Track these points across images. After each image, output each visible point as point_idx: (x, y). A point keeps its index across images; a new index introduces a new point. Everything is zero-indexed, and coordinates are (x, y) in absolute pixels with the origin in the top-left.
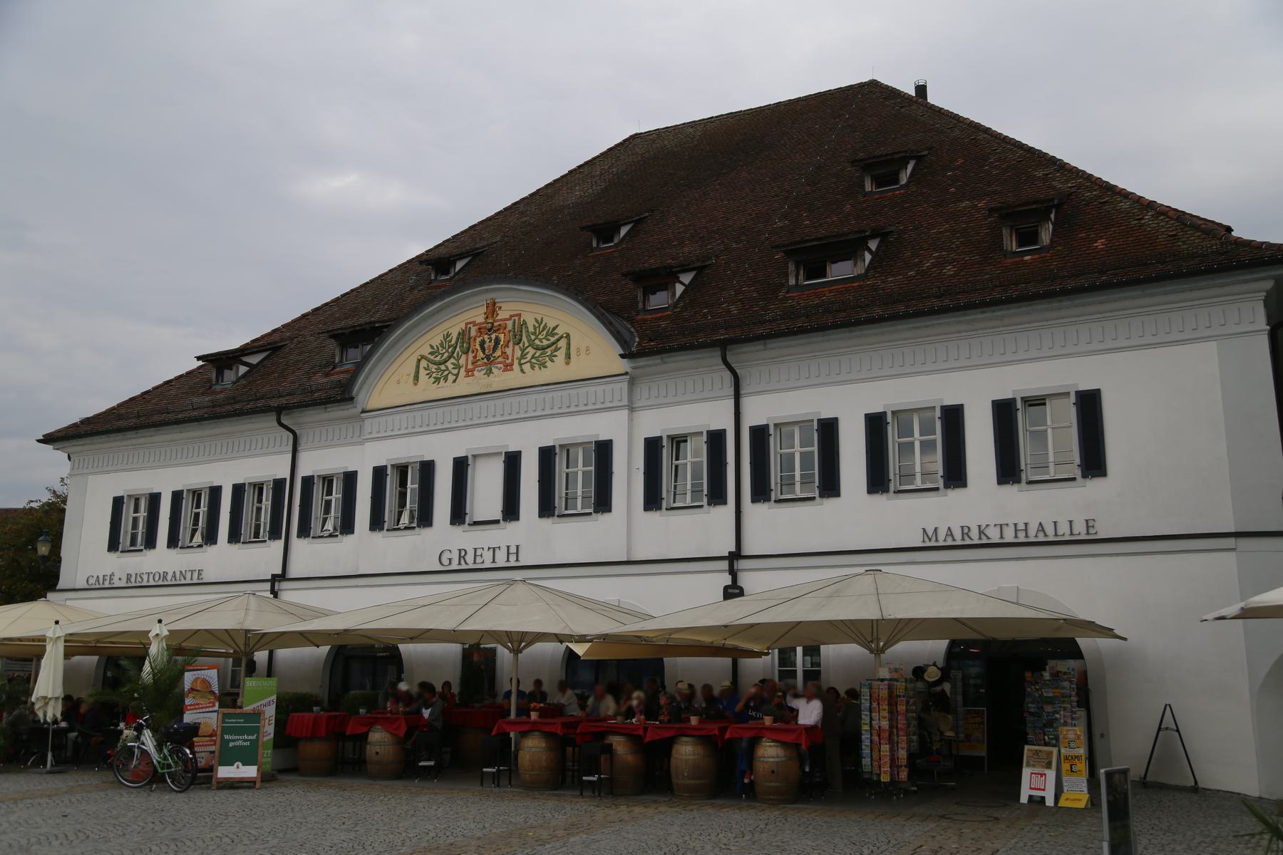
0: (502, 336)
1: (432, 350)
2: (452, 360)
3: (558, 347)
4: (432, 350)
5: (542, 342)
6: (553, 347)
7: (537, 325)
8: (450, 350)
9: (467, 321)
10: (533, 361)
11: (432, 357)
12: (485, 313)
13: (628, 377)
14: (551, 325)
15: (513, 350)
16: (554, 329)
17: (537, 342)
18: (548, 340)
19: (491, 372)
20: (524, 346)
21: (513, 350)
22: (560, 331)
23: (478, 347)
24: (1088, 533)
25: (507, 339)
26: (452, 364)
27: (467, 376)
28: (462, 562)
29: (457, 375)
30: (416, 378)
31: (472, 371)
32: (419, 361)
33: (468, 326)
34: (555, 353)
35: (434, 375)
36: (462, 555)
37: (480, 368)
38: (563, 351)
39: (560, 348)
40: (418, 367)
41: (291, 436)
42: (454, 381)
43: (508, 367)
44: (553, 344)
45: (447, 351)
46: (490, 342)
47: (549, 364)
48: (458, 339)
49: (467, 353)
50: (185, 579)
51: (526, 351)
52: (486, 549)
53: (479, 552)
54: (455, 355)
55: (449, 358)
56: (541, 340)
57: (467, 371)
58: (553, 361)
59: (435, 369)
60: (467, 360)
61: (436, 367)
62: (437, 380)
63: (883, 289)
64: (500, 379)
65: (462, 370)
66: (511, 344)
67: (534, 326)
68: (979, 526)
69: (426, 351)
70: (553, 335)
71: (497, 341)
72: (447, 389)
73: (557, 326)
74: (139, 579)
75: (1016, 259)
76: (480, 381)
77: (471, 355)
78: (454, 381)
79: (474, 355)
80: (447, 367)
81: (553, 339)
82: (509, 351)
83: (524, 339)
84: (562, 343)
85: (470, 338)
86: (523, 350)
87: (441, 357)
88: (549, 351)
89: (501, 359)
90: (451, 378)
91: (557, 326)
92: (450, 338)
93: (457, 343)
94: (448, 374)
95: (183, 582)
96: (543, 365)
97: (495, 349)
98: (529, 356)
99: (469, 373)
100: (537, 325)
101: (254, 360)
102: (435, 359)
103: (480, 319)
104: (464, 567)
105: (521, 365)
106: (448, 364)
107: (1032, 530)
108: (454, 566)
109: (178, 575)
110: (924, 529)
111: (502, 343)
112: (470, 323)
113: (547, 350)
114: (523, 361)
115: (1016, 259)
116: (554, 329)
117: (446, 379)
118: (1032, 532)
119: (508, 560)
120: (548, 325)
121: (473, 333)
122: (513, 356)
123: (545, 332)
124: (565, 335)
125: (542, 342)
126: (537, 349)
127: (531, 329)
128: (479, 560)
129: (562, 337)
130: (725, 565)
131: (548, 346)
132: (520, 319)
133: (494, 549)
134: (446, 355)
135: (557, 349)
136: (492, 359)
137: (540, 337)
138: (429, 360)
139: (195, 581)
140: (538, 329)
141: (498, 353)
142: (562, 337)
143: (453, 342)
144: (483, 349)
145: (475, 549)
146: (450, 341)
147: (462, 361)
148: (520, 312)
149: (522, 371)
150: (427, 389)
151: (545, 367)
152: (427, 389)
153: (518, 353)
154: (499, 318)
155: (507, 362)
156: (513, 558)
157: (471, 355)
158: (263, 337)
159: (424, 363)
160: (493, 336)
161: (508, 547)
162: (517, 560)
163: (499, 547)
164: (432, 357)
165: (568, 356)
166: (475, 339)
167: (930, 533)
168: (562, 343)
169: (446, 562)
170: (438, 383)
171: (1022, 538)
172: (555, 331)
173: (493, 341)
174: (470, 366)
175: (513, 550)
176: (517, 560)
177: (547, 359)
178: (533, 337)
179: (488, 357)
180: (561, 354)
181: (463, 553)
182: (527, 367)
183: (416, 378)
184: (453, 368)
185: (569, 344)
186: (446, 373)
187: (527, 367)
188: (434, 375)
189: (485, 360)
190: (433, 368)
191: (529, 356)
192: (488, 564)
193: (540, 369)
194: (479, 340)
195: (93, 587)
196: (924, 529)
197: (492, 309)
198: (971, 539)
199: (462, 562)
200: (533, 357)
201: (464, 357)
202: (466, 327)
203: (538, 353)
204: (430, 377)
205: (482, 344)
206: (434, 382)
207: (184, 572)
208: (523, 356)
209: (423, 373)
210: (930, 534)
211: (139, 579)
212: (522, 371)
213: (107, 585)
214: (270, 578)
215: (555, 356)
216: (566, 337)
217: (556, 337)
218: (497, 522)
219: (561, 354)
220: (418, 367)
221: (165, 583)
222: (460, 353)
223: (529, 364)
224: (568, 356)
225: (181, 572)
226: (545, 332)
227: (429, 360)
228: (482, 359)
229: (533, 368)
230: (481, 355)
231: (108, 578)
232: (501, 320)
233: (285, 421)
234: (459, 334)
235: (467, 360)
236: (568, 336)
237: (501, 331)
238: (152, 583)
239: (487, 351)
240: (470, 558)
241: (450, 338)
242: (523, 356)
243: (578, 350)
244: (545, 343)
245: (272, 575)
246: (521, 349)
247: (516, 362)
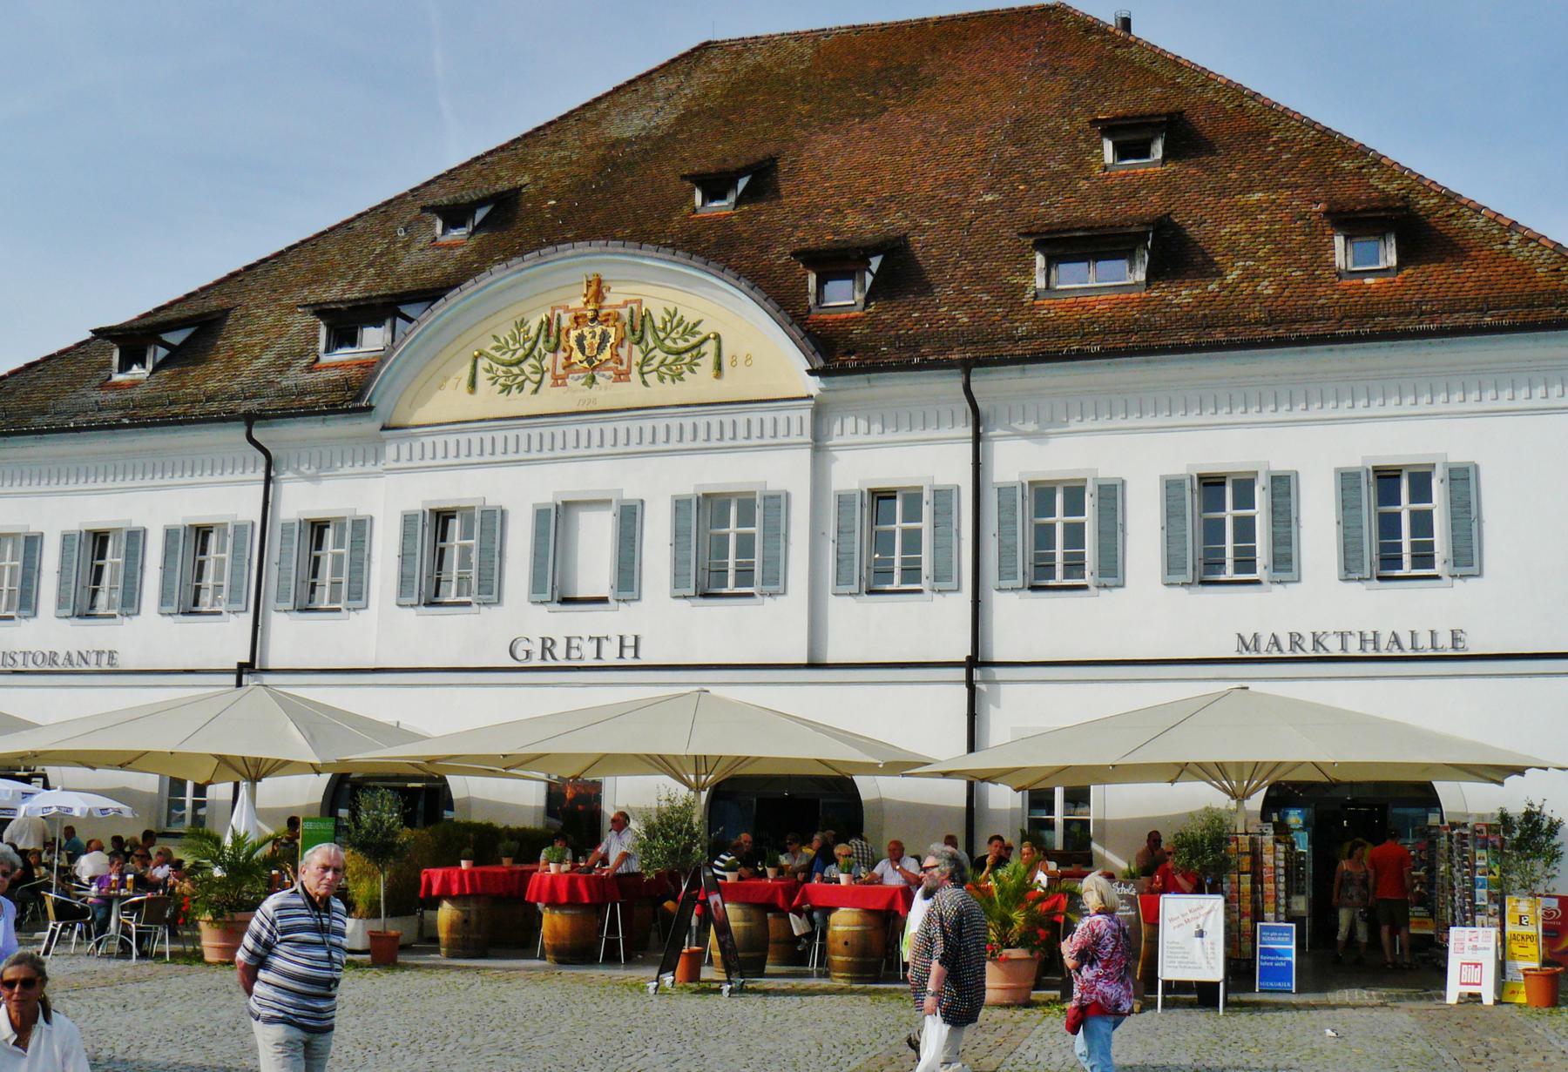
0: (612, 331)
1: (495, 344)
2: (531, 361)
3: (702, 351)
4: (495, 344)
5: (675, 343)
6: (694, 352)
7: (667, 318)
8: (528, 345)
9: (555, 305)
10: (663, 369)
11: (498, 355)
12: (586, 296)
13: (813, 402)
14: (690, 319)
15: (630, 352)
16: (695, 325)
17: (668, 343)
18: (687, 341)
19: (593, 379)
20: (647, 346)
21: (630, 352)
22: (704, 330)
23: (573, 343)
24: (1454, 647)
25: (621, 335)
26: (533, 366)
27: (555, 385)
28: (548, 656)
29: (540, 383)
30: (473, 384)
31: (563, 378)
32: (475, 359)
33: (557, 312)
34: (696, 361)
35: (502, 381)
36: (547, 647)
37: (576, 375)
39: (704, 355)
40: (474, 367)
41: (262, 458)
42: (536, 391)
43: (621, 376)
44: (694, 347)
45: (522, 347)
46: (594, 337)
47: (687, 375)
48: (540, 330)
49: (555, 351)
50: (86, 663)
51: (651, 355)
52: (586, 638)
53: (574, 643)
54: (536, 353)
55: (527, 357)
56: (674, 341)
57: (556, 378)
58: (692, 371)
59: (503, 372)
60: (555, 362)
61: (504, 368)
62: (507, 389)
63: (1178, 305)
64: (607, 392)
65: (548, 376)
66: (627, 344)
67: (663, 319)
68: (1314, 634)
70: (693, 334)
71: (604, 337)
73: (699, 322)
75: (1355, 282)
76: (574, 394)
77: (561, 356)
78: (536, 391)
79: (566, 355)
80: (523, 372)
81: (693, 341)
82: (623, 352)
83: (649, 337)
84: (709, 347)
85: (559, 330)
86: (646, 354)
87: (513, 355)
88: (687, 357)
89: (611, 364)
90: (529, 386)
91: (699, 322)
92: (526, 328)
93: (538, 336)
94: (524, 381)
95: (85, 667)
96: (678, 377)
97: (601, 348)
98: (655, 363)
99: (558, 381)
100: (667, 318)
101: (176, 338)
102: (503, 357)
103: (578, 303)
104: (550, 662)
105: (642, 374)
106: (525, 366)
107: (1384, 642)
108: (536, 661)
109: (75, 657)
110: (1239, 635)
111: (612, 340)
112: (559, 307)
113: (683, 356)
114: (646, 369)
115: (1355, 282)
116: (695, 325)
117: (521, 387)
118: (1383, 644)
119: (621, 656)
120: (686, 320)
121: (566, 321)
122: (630, 360)
123: (681, 329)
124: (712, 336)
125: (675, 343)
126: (669, 352)
127: (659, 324)
128: (574, 654)
129: (707, 339)
130: (961, 673)
131: (687, 351)
132: (640, 307)
133: (599, 640)
134: (520, 353)
136: (597, 363)
137: (673, 335)
138: (492, 358)
139: (105, 667)
140: (669, 325)
141: (607, 354)
142: (707, 339)
143: (533, 333)
144: (582, 349)
145: (569, 639)
146: (527, 332)
147: (548, 362)
148: (639, 297)
149: (645, 383)
150: (489, 400)
151: (682, 379)
152: (489, 400)
153: (638, 356)
154: (605, 303)
155: (620, 368)
156: (629, 653)
157: (561, 356)
158: (172, 304)
159: (483, 363)
160: (598, 330)
161: (621, 638)
162: (636, 656)
163: (607, 638)
164: (498, 355)
165: (719, 367)
166: (568, 332)
167: (1248, 639)
168: (709, 347)
169: (521, 655)
170: (509, 393)
171: (1370, 652)
172: (697, 329)
173: (597, 337)
174: (560, 371)
175: (630, 642)
176: (636, 656)
177: (685, 368)
178: (662, 335)
179: (590, 360)
180: (707, 363)
181: (549, 643)
182: (652, 378)
183: (473, 384)
184: (532, 373)
185: (719, 349)
186: (521, 379)
187: (652, 378)
188: (502, 381)
189: (585, 364)
191: (655, 363)
192: (590, 660)
193: (674, 381)
194: (574, 334)
196: (1239, 635)
197: (597, 290)
198: (1303, 650)
199: (548, 656)
200: (662, 363)
201: (550, 356)
202: (553, 314)
203: (671, 358)
204: (495, 383)
205: (580, 340)
206: (502, 391)
207: (85, 654)
208: (646, 361)
209: (482, 376)
210: (1248, 642)
212: (645, 383)
214: (235, 667)
215: (696, 365)
216: (714, 338)
217: (699, 338)
218: (604, 600)
219: (707, 363)
220: (474, 367)
221: (55, 668)
222: (543, 351)
223: (655, 373)
224: (719, 367)
225: (79, 653)
226: (681, 329)
227: (492, 358)
228: (581, 362)
229: (662, 379)
230: (577, 356)
232: (610, 307)
233: (257, 434)
234: (542, 322)
235: (555, 362)
236: (717, 337)
237: (611, 323)
238: (32, 667)
239: (587, 352)
240: (560, 651)
241: (526, 328)
242: (646, 361)
243: (734, 359)
244: (681, 344)
246: (643, 352)
247: (635, 369)
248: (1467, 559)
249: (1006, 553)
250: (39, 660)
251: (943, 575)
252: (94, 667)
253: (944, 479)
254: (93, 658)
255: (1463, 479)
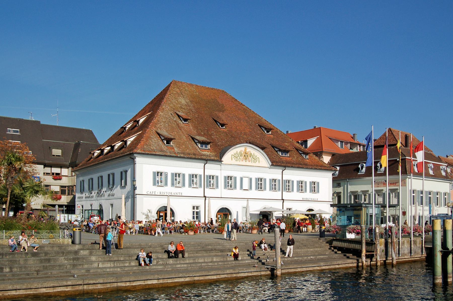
14: (256, 155)
22: (258, 157)
30: (232, 159)
38: (258, 161)
57: (242, 160)
64: (248, 163)
65: (241, 160)
69: (233, 154)
72: (238, 163)
74: (163, 193)
76: (244, 163)
84: (258, 159)
88: (256, 160)
90: (239, 161)
95: (177, 195)
96: (255, 162)
99: (242, 161)
109: (175, 193)
135: (257, 160)
139: (180, 195)
143: (239, 153)
150: (234, 162)
152: (234, 162)
168: (258, 159)
174: (242, 159)
183: (232, 159)
190: (235, 158)
195: (149, 194)
209: (233, 158)
211: (163, 193)
213: (153, 194)
218: (247, 190)
219: (258, 161)
221: (172, 195)
230: (244, 158)
231: (154, 193)
245: (331, 207)
248: (318, 192)
249: (285, 188)
250: (169, 193)
251: (279, 190)
252: (178, 195)
253: (279, 179)
254: (178, 194)
255: (318, 183)
